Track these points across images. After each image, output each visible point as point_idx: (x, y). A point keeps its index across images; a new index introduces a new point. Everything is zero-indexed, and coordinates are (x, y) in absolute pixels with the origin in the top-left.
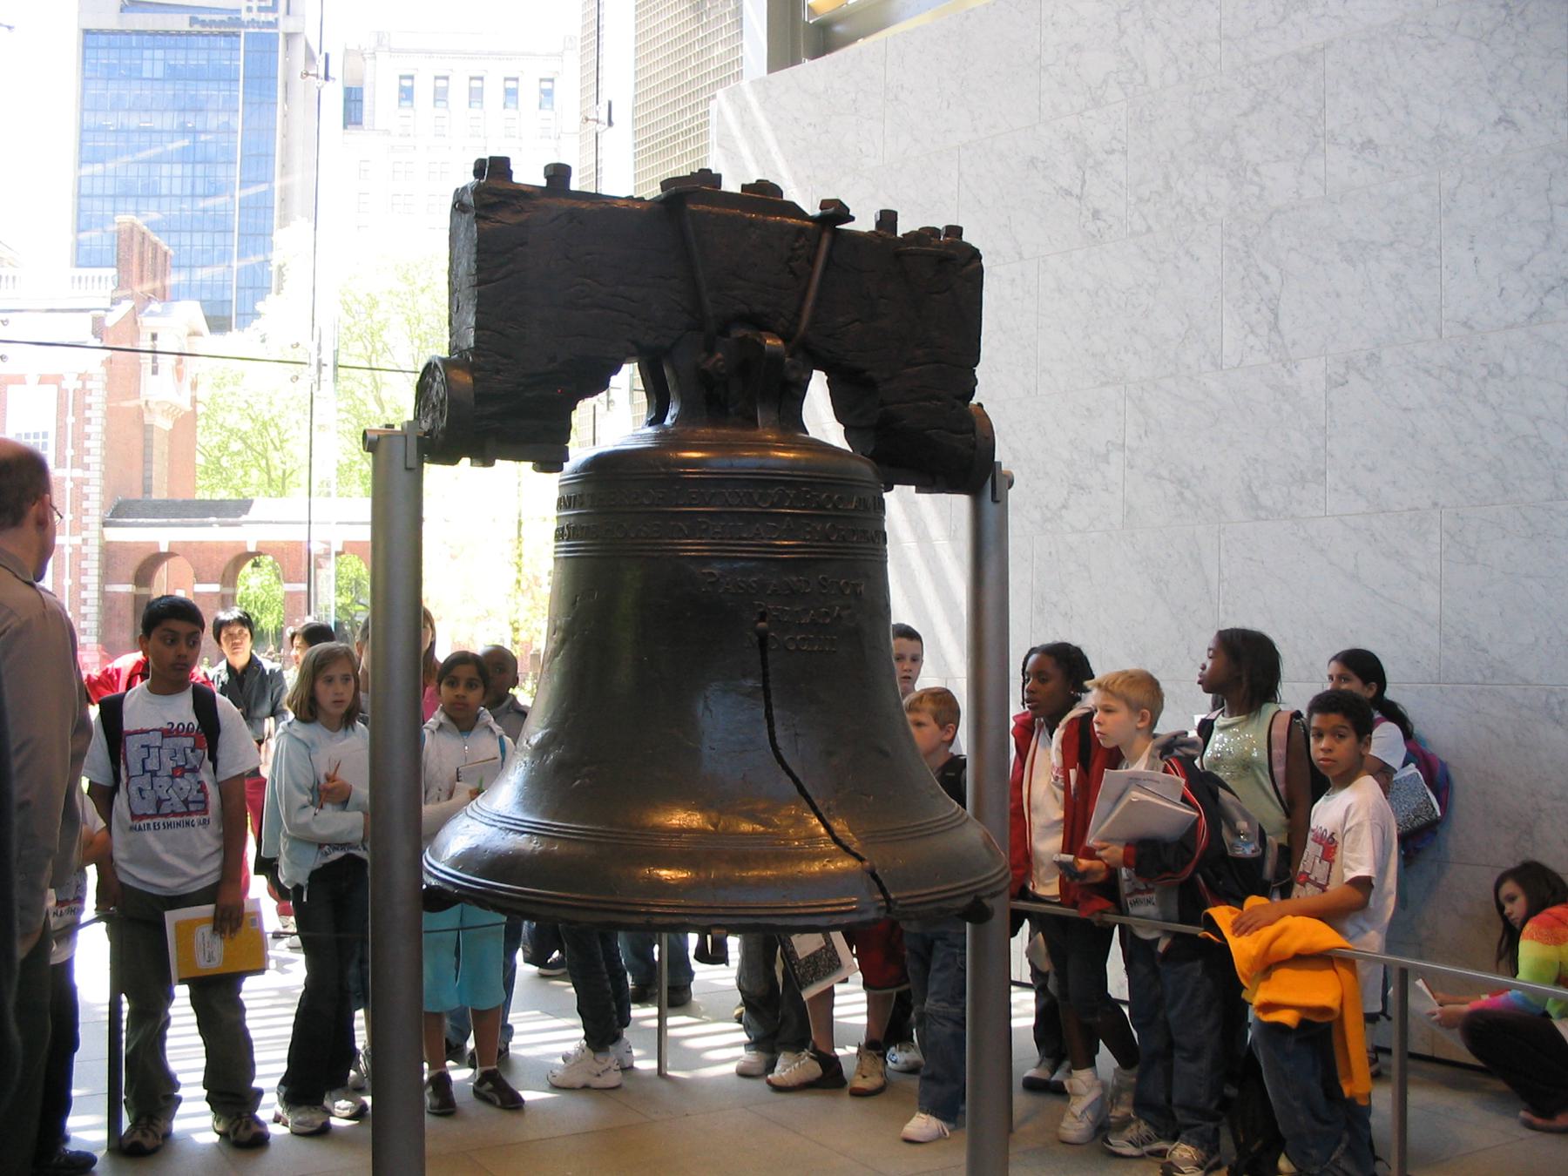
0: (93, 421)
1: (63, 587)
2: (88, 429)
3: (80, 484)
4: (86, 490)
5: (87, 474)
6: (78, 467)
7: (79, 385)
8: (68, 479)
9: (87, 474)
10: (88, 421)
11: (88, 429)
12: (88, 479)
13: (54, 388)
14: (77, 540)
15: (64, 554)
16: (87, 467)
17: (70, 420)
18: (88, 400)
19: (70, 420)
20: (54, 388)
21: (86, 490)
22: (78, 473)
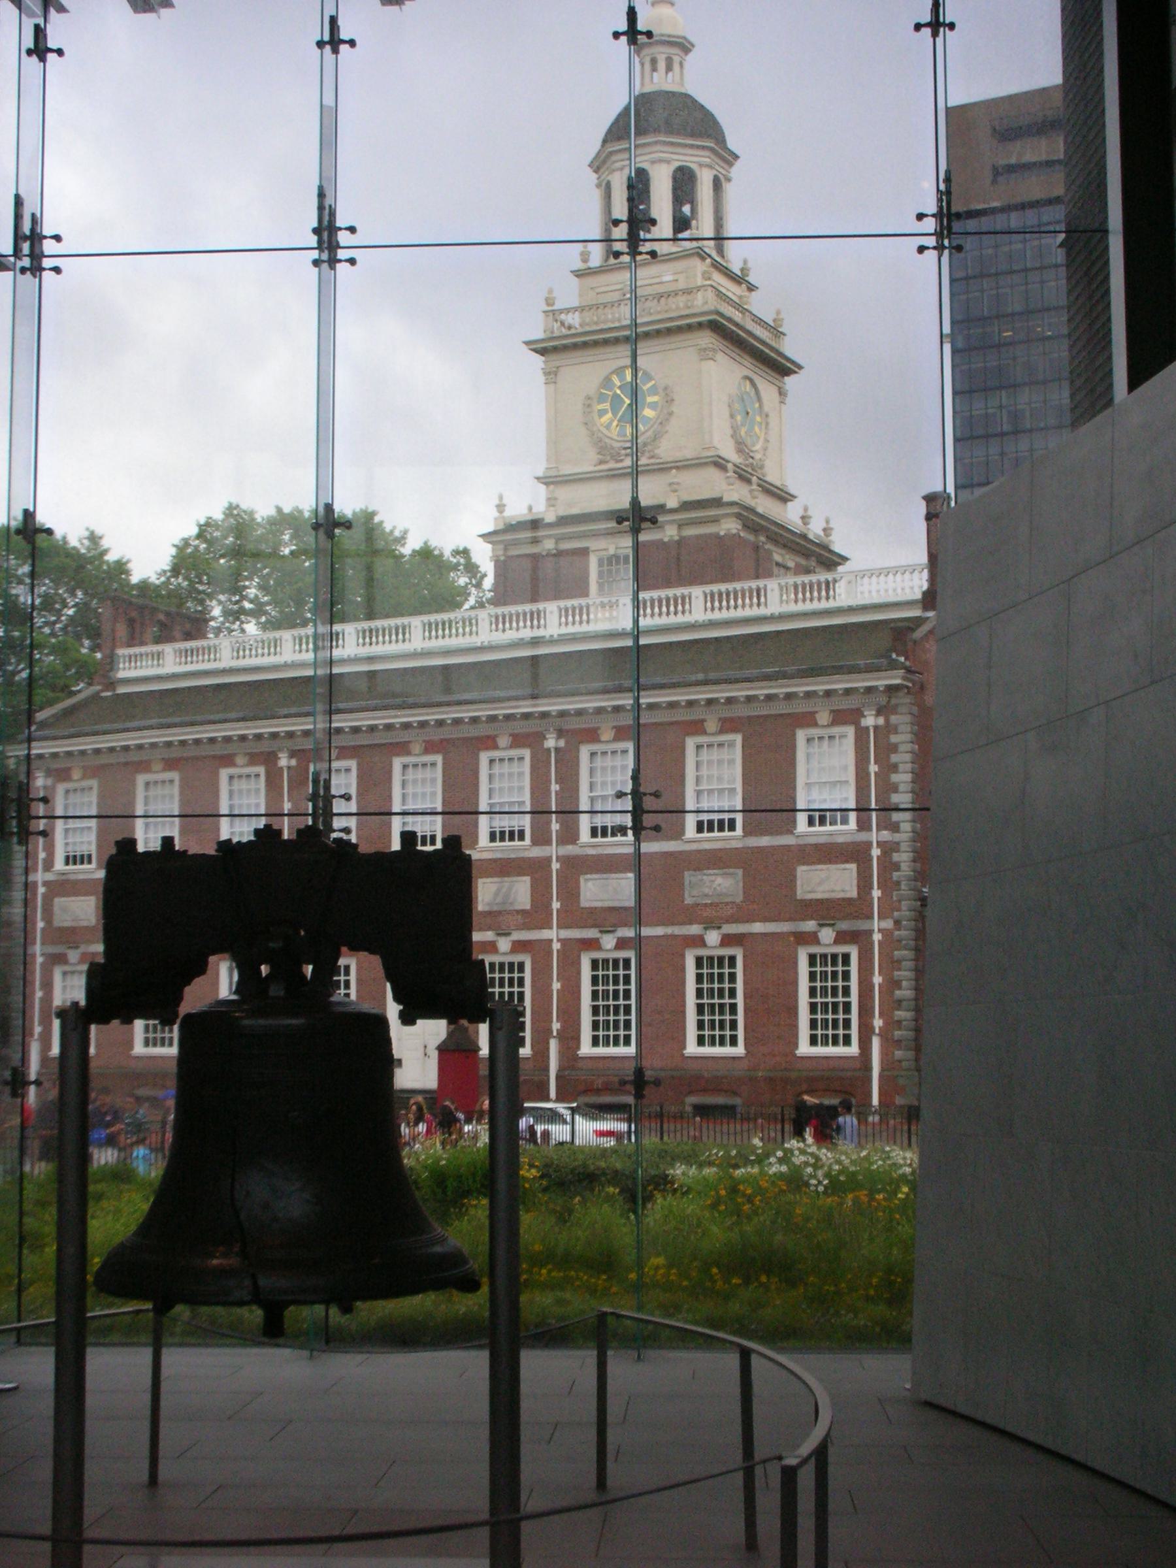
0: (901, 767)
1: (873, 986)
2: (895, 778)
3: (888, 849)
4: (896, 857)
5: (897, 837)
6: (886, 828)
7: (881, 721)
8: (875, 844)
9: (897, 837)
10: (894, 768)
11: (895, 778)
12: (898, 843)
13: (850, 731)
14: (888, 924)
15: (872, 943)
16: (895, 828)
17: (873, 768)
18: (894, 739)
19: (873, 768)
20: (850, 731)
21: (896, 857)
22: (886, 835)
